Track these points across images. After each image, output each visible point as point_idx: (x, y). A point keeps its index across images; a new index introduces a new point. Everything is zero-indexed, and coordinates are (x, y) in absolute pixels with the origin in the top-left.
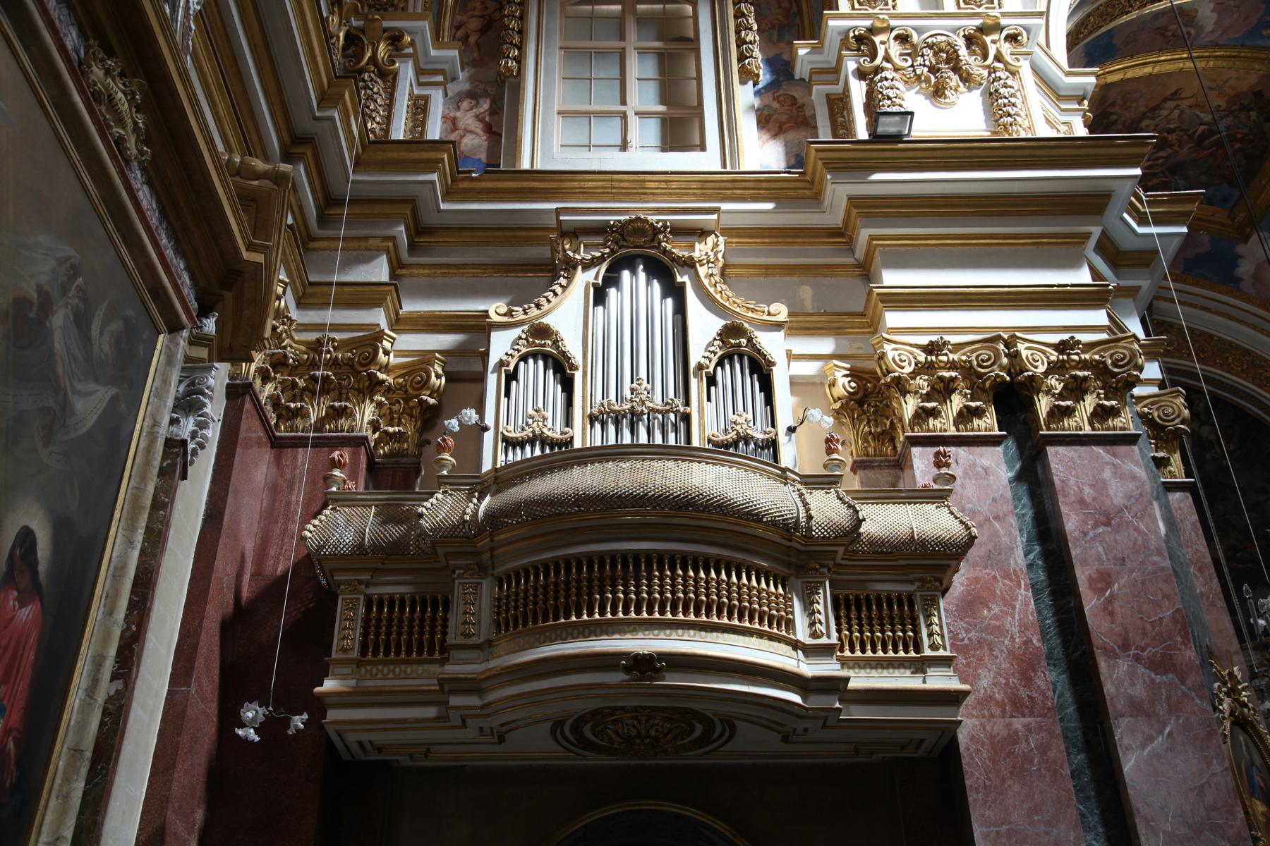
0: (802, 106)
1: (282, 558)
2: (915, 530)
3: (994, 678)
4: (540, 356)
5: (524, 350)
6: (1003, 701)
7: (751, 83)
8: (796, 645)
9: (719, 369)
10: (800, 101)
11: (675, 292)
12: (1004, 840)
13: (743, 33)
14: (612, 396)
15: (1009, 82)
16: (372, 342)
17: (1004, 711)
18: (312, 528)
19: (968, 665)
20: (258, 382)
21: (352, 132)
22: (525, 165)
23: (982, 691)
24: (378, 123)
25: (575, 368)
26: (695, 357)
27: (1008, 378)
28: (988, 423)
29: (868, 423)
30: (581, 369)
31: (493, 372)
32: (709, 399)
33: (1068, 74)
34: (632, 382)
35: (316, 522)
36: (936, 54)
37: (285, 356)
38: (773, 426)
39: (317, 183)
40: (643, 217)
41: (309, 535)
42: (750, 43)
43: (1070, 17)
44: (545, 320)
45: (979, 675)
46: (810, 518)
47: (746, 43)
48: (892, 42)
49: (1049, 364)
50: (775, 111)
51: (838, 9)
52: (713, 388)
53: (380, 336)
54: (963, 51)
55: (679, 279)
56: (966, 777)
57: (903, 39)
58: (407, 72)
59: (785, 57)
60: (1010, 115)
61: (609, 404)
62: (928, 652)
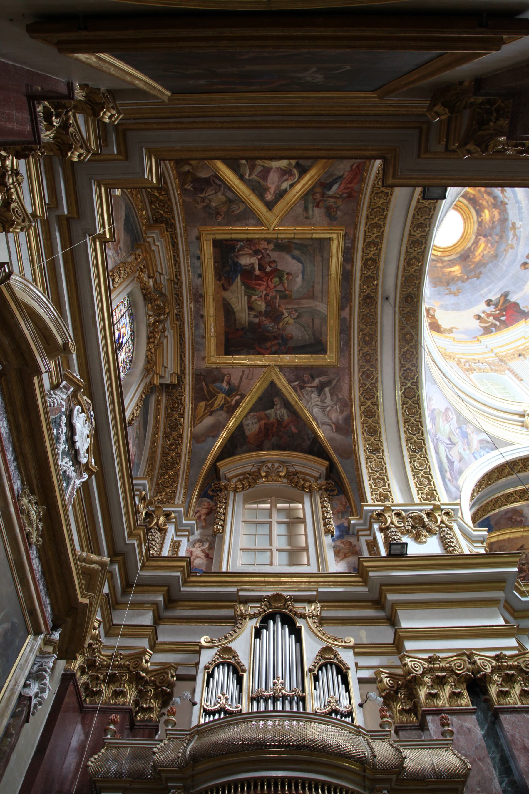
0: (355, 546)
2: (435, 765)
4: (226, 665)
7: (330, 536)
9: (320, 672)
10: (353, 544)
11: (296, 632)
13: (326, 515)
14: (263, 687)
15: (449, 532)
20: (78, 674)
21: (142, 552)
22: (224, 570)
24: (156, 551)
26: (307, 666)
27: (472, 676)
28: (465, 701)
29: (402, 703)
32: (315, 689)
33: (474, 531)
34: (274, 679)
35: (96, 756)
36: (413, 521)
37: (95, 661)
38: (350, 703)
39: (123, 575)
40: (280, 593)
41: (91, 764)
42: (329, 518)
43: (471, 508)
44: (229, 645)
47: (327, 518)
48: (393, 516)
49: (492, 667)
50: (342, 548)
51: (367, 502)
52: (317, 683)
53: (144, 652)
54: (426, 519)
55: (298, 625)
57: (398, 514)
58: (171, 529)
59: (346, 524)
60: (451, 546)
61: (261, 691)
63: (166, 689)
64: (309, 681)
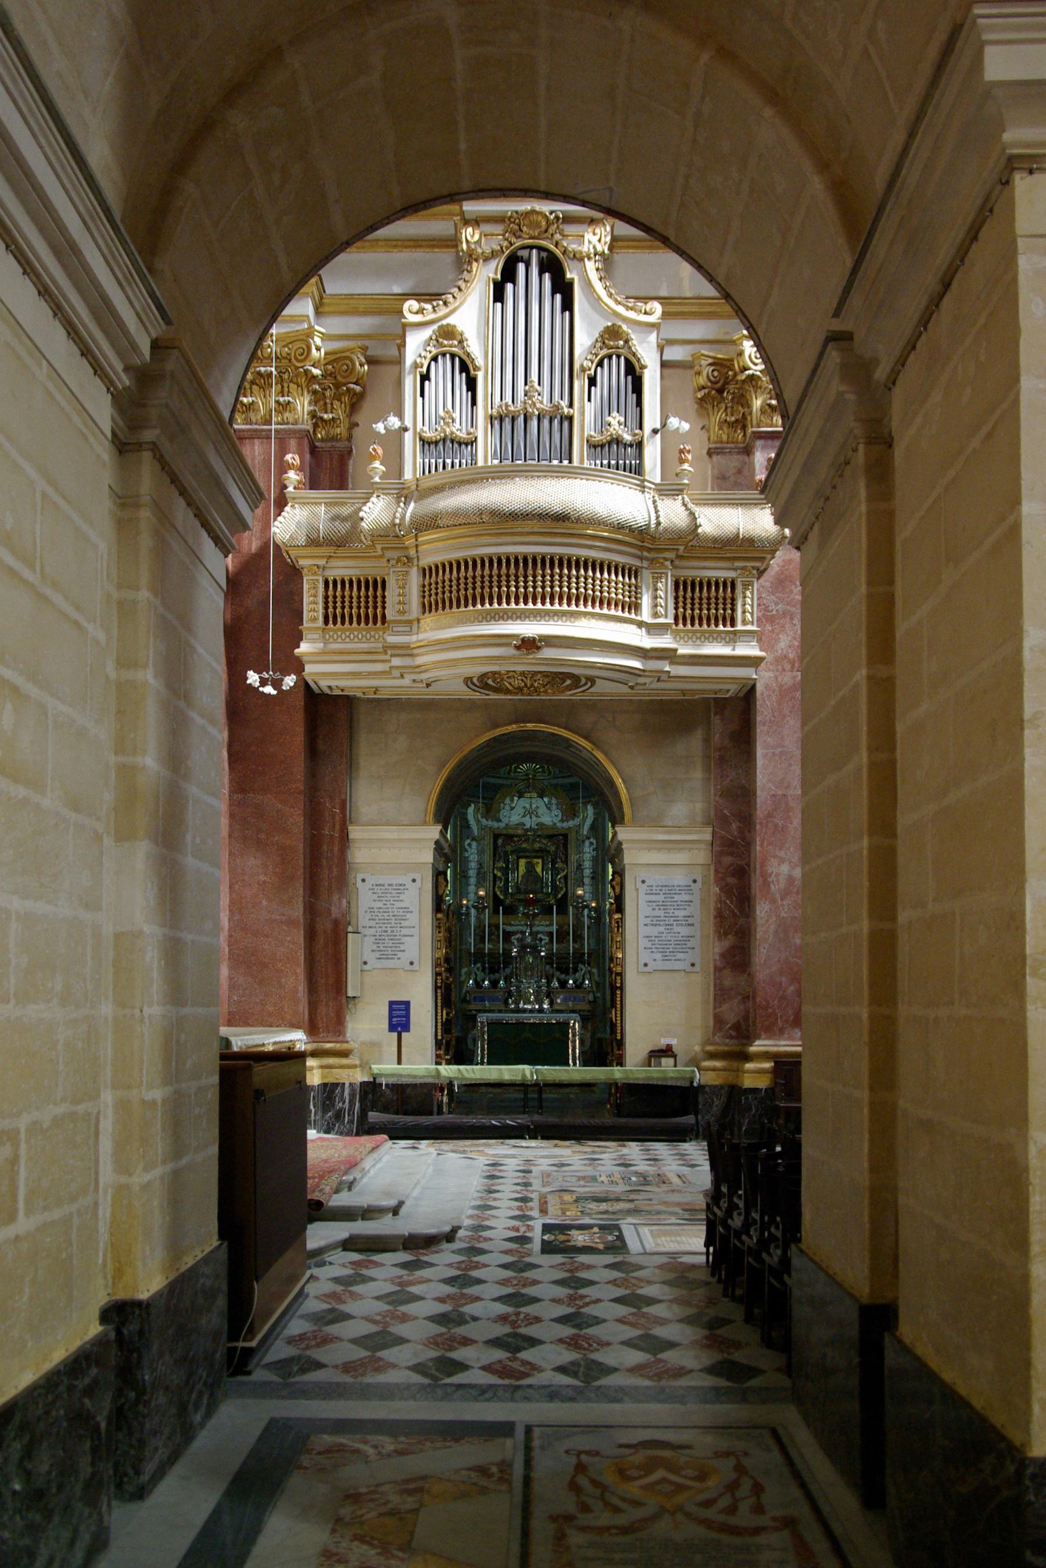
1: (254, 539)
2: (741, 530)
3: (791, 641)
5: (434, 351)
6: (794, 659)
8: (640, 624)
9: (599, 368)
12: (777, 758)
14: (508, 399)
16: (304, 337)
17: (793, 667)
18: (280, 525)
19: (772, 631)
23: (780, 651)
25: (477, 369)
30: (483, 369)
31: (409, 374)
38: (641, 428)
45: (779, 639)
46: (658, 524)
56: (758, 714)
61: (507, 405)
62: (739, 627)
63: (355, 386)
64: (580, 385)
